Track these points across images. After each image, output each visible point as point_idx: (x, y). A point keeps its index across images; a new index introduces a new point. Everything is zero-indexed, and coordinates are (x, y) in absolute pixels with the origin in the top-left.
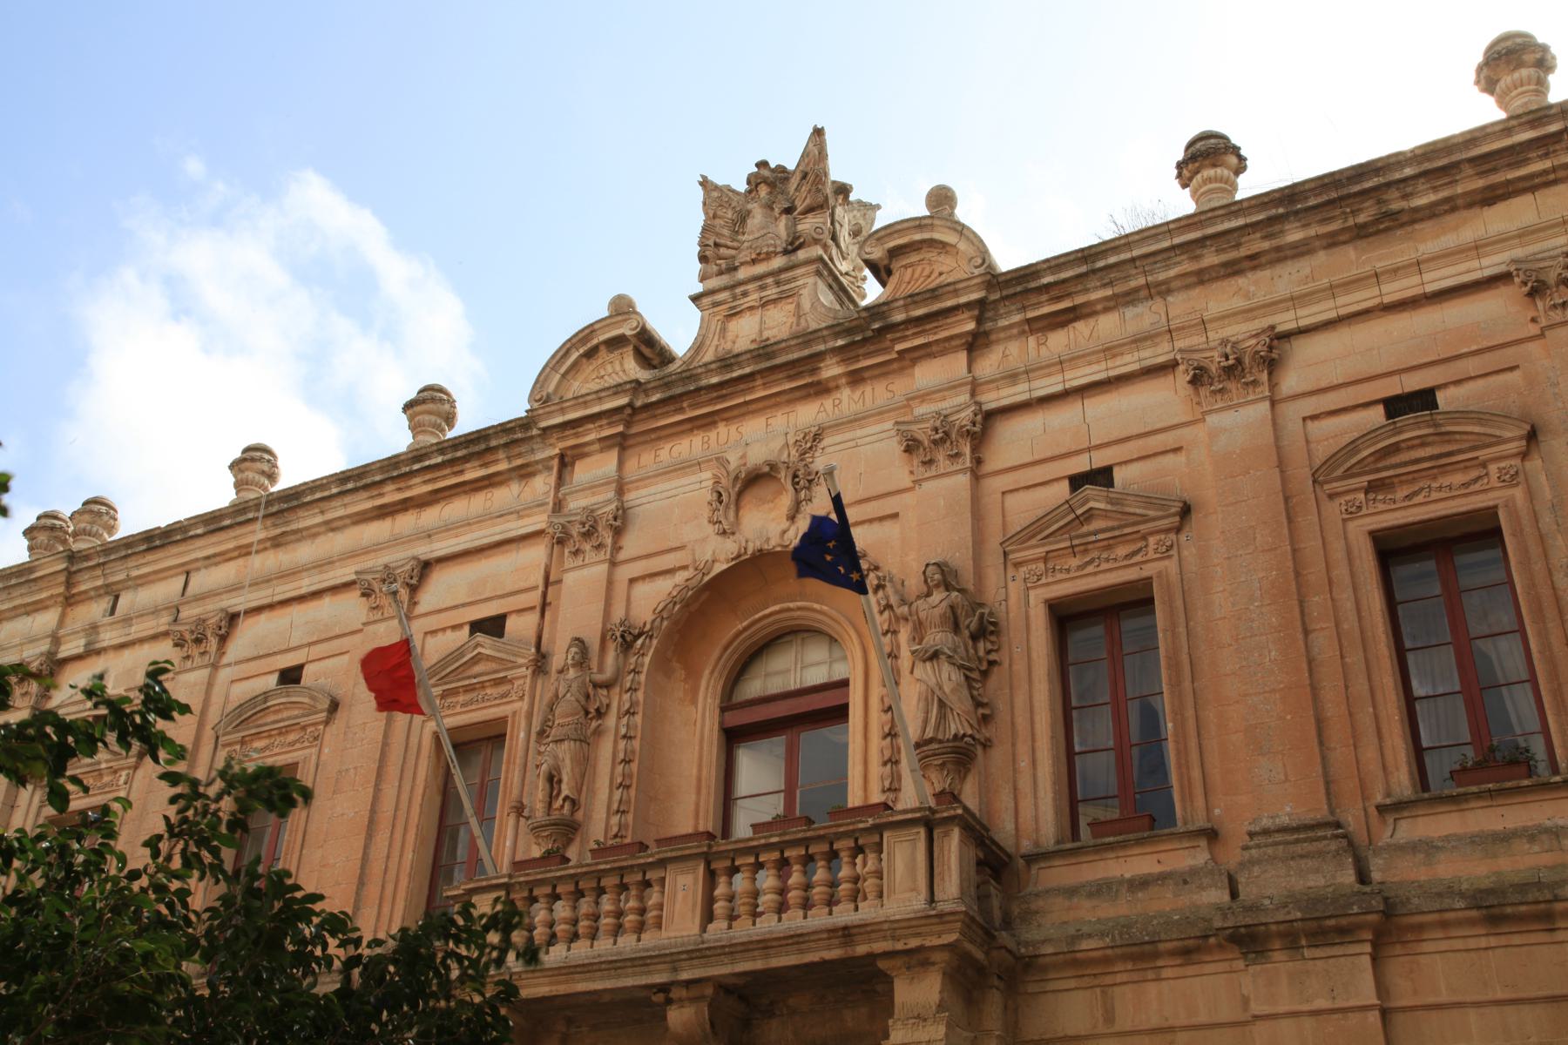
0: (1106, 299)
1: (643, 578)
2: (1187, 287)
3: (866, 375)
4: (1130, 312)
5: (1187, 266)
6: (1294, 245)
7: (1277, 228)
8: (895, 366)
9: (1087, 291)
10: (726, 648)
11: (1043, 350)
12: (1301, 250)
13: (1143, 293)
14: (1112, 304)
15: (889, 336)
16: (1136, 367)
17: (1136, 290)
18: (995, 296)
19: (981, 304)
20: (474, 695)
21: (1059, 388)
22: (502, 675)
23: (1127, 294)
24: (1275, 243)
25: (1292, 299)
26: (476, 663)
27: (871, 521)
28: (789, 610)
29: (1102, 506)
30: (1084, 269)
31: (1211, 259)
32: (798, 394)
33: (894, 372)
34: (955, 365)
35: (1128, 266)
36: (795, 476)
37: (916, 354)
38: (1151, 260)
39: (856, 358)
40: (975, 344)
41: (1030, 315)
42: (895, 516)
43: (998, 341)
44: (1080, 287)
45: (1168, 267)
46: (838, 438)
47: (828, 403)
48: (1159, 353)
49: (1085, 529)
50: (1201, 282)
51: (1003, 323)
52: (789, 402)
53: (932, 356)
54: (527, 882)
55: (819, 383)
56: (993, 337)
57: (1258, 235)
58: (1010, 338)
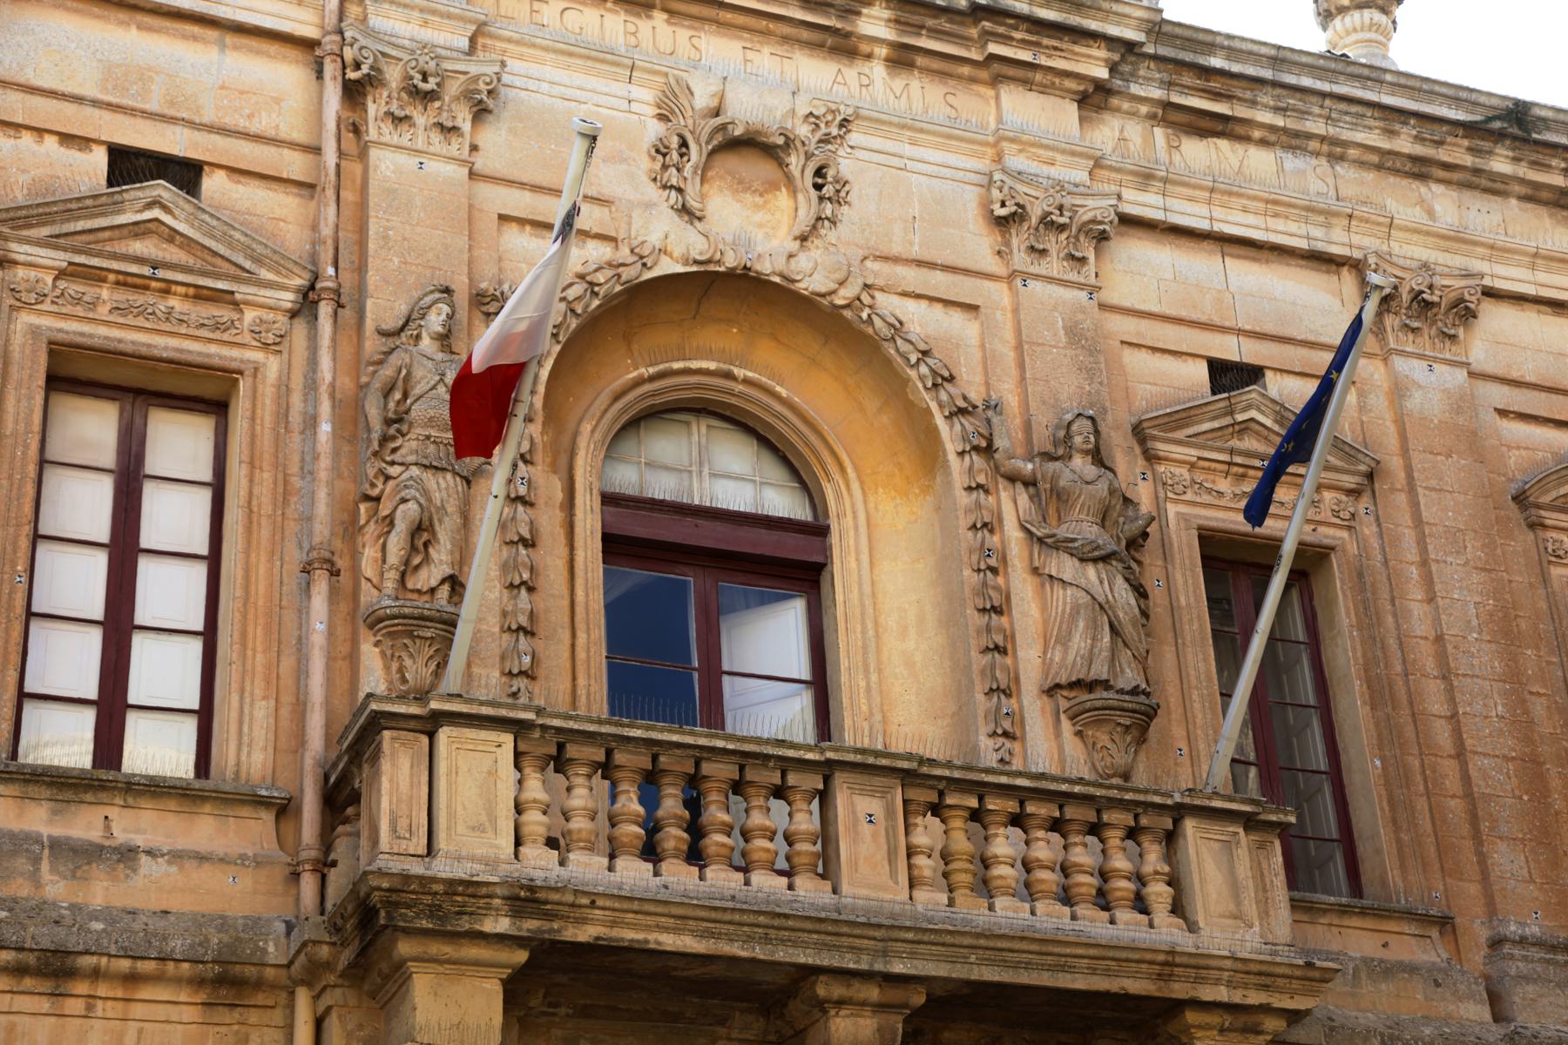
0: (1273, 129)
1: (522, 222)
2: (1362, 164)
3: (920, 60)
4: (1292, 162)
5: (1374, 139)
6: (1494, 176)
7: (1486, 145)
8: (965, 70)
9: (1253, 103)
10: (617, 398)
11: (1177, 158)
12: (1495, 187)
13: (1314, 145)
14: (1273, 138)
15: (987, 24)
16: (1302, 244)
17: (1309, 136)
18: (1149, 49)
19: (1130, 47)
20: (139, 299)
21: (1204, 225)
22: (221, 285)
23: (1297, 134)
24: (1479, 162)
25: (1492, 247)
26: (136, 236)
27: (932, 299)
28: (729, 376)
29: (1268, 422)
30: (1267, 74)
31: (1405, 143)
32: (805, 34)
33: (959, 77)
34: (1055, 116)
35: (1314, 99)
36: (819, 172)
37: (1011, 71)
38: (1343, 106)
39: (918, 29)
40: (1094, 98)
41: (1177, 99)
42: (972, 308)
43: (1118, 110)
44: (1248, 95)
45: (1354, 126)
46: (876, 142)
47: (852, 73)
48: (1337, 241)
49: (1235, 443)
50: (1379, 167)
51: (1135, 89)
52: (786, 39)
53: (1028, 84)
54: (559, 730)
55: (848, 35)
56: (1115, 101)
57: (1466, 143)
58: (1133, 114)
